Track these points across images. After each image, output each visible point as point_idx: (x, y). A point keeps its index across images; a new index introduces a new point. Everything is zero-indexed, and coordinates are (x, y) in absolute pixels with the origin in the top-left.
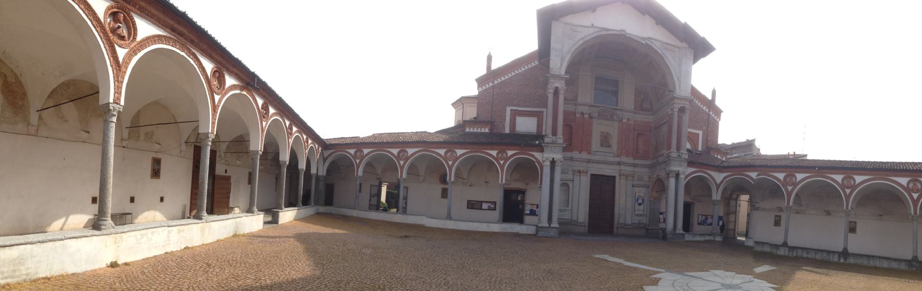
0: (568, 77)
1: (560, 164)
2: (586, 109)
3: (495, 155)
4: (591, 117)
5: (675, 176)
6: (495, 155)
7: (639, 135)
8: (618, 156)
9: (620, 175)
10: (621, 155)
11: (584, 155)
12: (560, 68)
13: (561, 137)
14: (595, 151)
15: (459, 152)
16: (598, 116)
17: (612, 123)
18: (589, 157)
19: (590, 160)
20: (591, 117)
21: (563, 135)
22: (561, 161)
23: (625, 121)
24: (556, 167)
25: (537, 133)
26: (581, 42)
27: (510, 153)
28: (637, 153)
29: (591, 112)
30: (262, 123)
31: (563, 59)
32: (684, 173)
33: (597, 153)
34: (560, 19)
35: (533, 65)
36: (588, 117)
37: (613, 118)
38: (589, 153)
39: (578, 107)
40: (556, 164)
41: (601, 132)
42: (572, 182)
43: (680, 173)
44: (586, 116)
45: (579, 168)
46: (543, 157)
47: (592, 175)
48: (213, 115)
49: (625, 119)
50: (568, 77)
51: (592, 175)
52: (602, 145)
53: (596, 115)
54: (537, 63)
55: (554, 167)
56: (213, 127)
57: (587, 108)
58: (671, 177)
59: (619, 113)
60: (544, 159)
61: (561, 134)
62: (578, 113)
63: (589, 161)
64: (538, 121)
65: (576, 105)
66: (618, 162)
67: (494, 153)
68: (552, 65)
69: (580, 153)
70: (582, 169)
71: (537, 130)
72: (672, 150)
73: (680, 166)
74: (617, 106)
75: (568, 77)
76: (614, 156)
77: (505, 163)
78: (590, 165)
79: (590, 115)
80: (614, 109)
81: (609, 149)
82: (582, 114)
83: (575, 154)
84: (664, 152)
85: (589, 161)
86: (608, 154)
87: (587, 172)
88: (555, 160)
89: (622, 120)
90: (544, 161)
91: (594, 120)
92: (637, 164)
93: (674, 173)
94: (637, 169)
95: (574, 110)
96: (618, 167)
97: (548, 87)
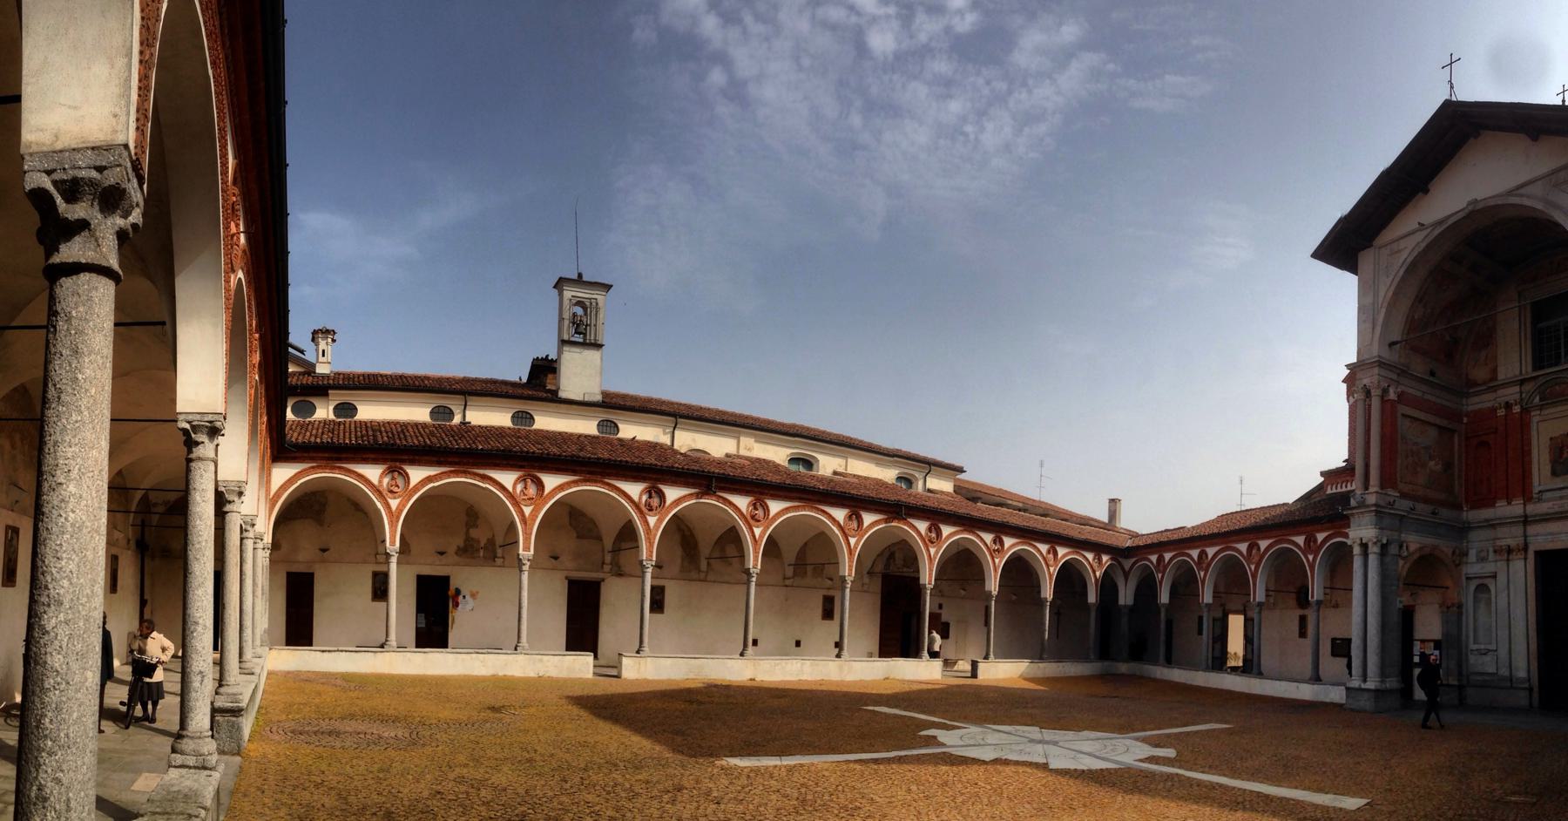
2: (1511, 394)
3: (1302, 544)
6: (1302, 544)
11: (1516, 508)
14: (1540, 492)
15: (1263, 544)
16: (1541, 400)
18: (1532, 509)
27: (1320, 537)
30: (928, 550)
39: (1500, 392)
41: (1551, 439)
42: (1492, 581)
44: (1517, 409)
47: (1537, 553)
48: (849, 558)
51: (1537, 553)
52: (1554, 473)
56: (850, 570)
63: (1526, 521)
67: (1300, 540)
70: (1512, 542)
77: (1314, 559)
78: (1531, 530)
82: (1508, 406)
83: (1503, 509)
85: (1526, 521)
87: (1526, 549)
91: (1532, 414)
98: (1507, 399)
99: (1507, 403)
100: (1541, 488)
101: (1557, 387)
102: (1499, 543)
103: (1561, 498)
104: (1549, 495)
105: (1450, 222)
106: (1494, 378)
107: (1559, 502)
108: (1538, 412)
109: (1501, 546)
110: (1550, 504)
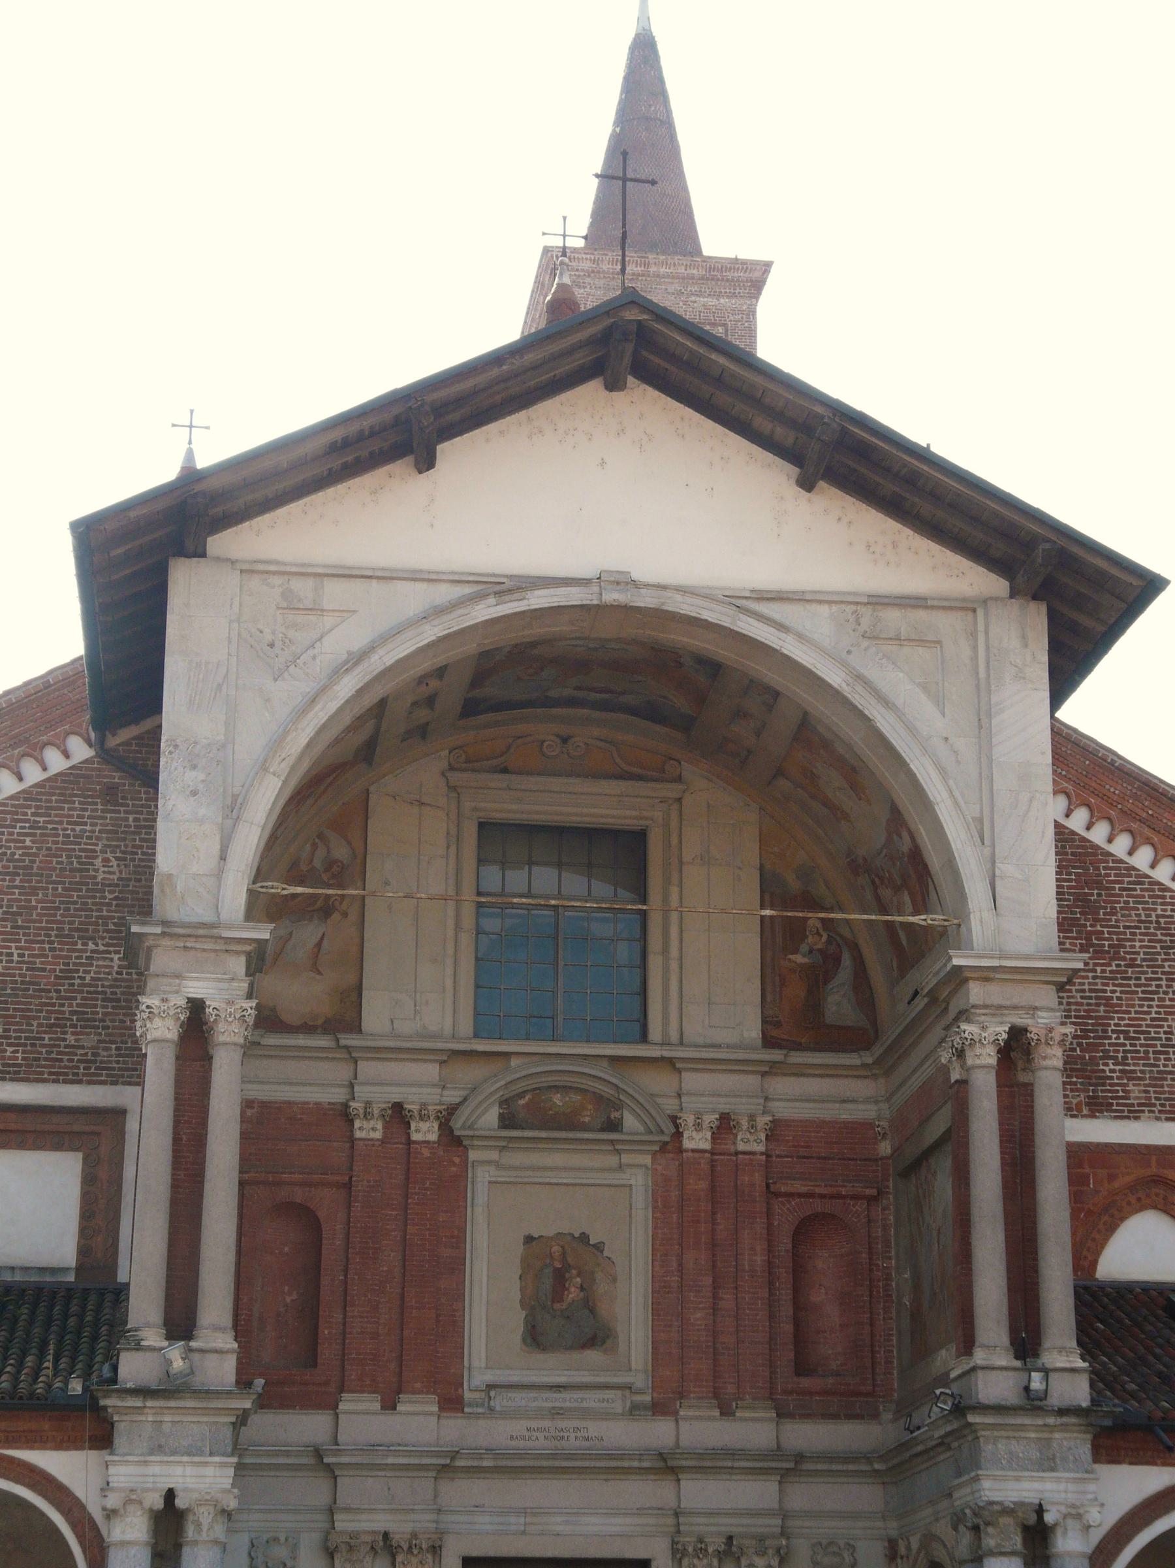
0: (267, 936)
1: (219, 1531)
4: (452, 1140)
5: (1017, 1541)
7: (805, 1230)
8: (659, 1408)
9: (674, 1551)
10: (681, 1395)
12: (219, 874)
13: (227, 1341)
14: (490, 1387)
16: (507, 1121)
17: (613, 1160)
19: (454, 1455)
20: (452, 1140)
21: (241, 1327)
22: (227, 1514)
23: (697, 1140)
24: (186, 1551)
25: (79, 1269)
26: (347, 687)
28: (802, 1368)
29: (452, 1096)
31: (234, 808)
32: (1076, 1514)
33: (500, 1401)
34: (218, 543)
35: (56, 762)
36: (433, 1137)
37: (613, 1126)
38: (452, 1403)
39: (367, 1069)
40: (190, 1532)
41: (529, 1239)
43: (1049, 1518)
44: (425, 1132)
45: (380, 1522)
46: (106, 1488)
49: (698, 1126)
50: (263, 932)
52: (535, 1338)
53: (491, 1117)
54: (80, 750)
55: (178, 1547)
57: (431, 1071)
58: (992, 1553)
59: (658, 1082)
60: (112, 1501)
61: (227, 1320)
62: (367, 1115)
64: (89, 1180)
65: (352, 1056)
66: (661, 1456)
68: (165, 860)
69: (389, 1405)
70: (400, 1527)
71: (84, 1251)
72: (980, 1357)
73: (1048, 1463)
74: (644, 1038)
75: (263, 932)
76: (634, 1410)
78: (456, 1492)
79: (446, 1118)
80: (614, 1060)
81: (593, 1356)
82: (398, 1115)
84: (945, 1359)
86: (592, 1400)
87: (436, 1550)
88: (180, 1503)
89: (678, 1135)
90: (110, 1514)
92: (800, 1457)
93: (1005, 1520)
94: (801, 1496)
95: (337, 1095)
96: (659, 1492)
97: (145, 1000)
98: (395, 1094)
99: (398, 1107)
100: (489, 1377)
101: (557, 1099)
102: (343, 1523)
103: (556, 1413)
104: (519, 1399)
105: (539, 599)
106: (355, 1027)
107: (546, 1423)
108: (494, 1155)
109: (354, 1535)
110: (519, 1427)
